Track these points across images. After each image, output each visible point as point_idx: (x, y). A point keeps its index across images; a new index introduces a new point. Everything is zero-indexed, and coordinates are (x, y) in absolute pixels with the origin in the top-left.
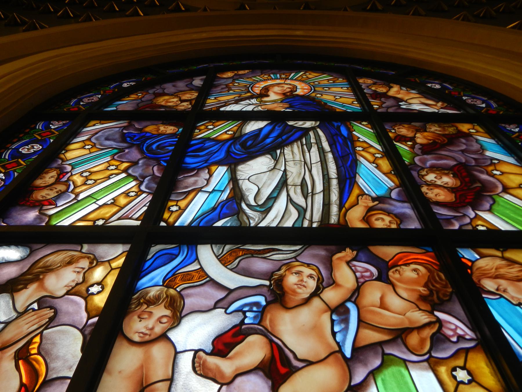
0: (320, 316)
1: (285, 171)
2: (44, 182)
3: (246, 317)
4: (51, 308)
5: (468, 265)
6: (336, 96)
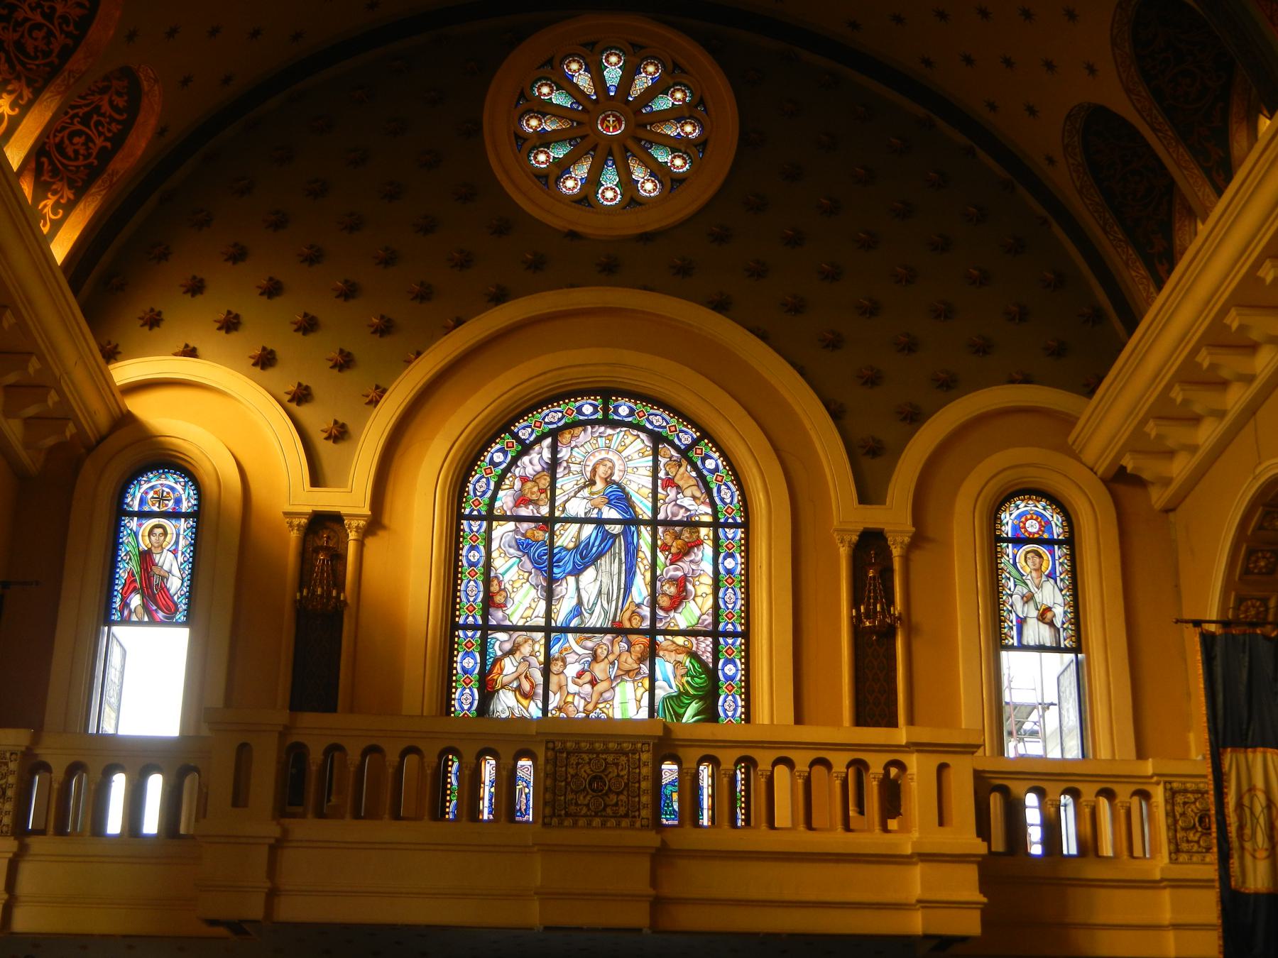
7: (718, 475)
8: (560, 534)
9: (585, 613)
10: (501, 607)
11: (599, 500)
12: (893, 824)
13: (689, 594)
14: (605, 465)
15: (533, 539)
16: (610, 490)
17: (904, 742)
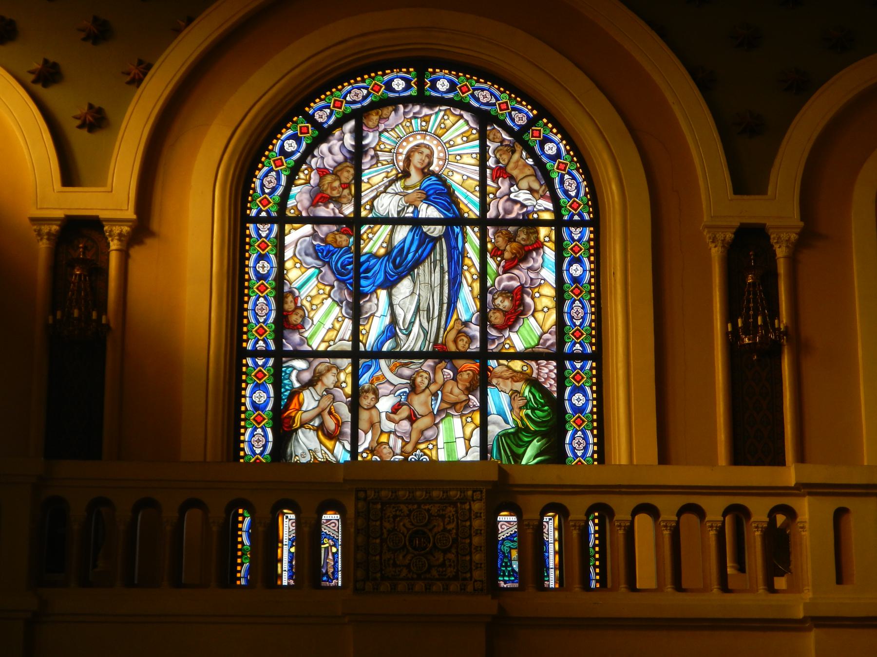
1: (419, 294)
4: (332, 394)
7: (559, 162)
8: (368, 238)
9: (400, 334)
10: (298, 329)
11: (415, 196)
12: (781, 583)
13: (527, 308)
14: (422, 153)
15: (334, 245)
16: (428, 183)
17: (792, 483)
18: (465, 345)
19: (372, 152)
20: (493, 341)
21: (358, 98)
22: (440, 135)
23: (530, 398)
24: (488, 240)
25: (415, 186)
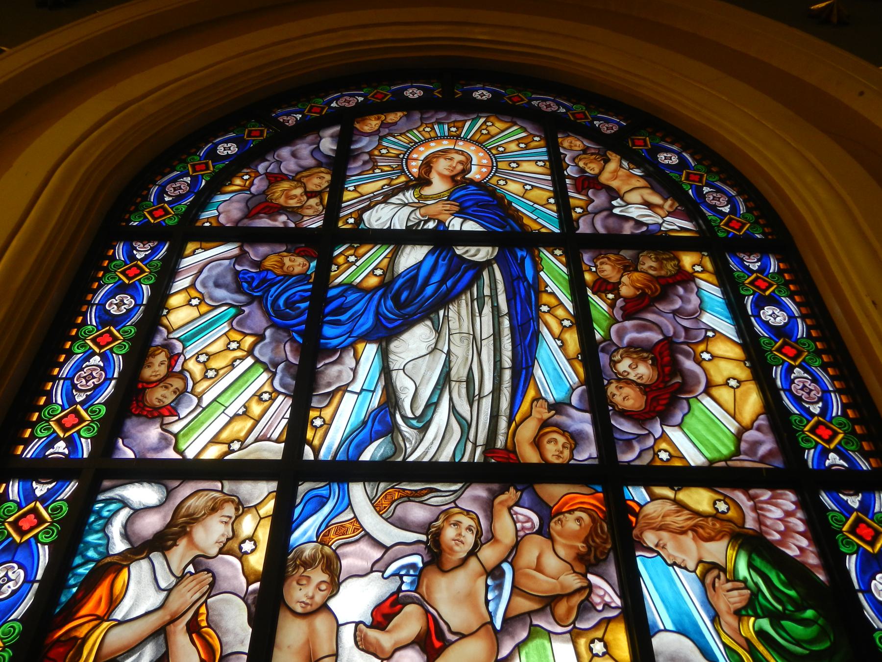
0: (475, 581)
1: (449, 351)
2: (154, 374)
3: (403, 582)
4: (209, 571)
5: (635, 511)
6: (527, 184)
9: (404, 427)
14: (451, 159)
15: (278, 271)
18: (562, 452)
19: (366, 157)
20: (628, 444)
21: (349, 104)
22: (481, 142)
23: (756, 584)
24: (584, 267)
25: (438, 196)
